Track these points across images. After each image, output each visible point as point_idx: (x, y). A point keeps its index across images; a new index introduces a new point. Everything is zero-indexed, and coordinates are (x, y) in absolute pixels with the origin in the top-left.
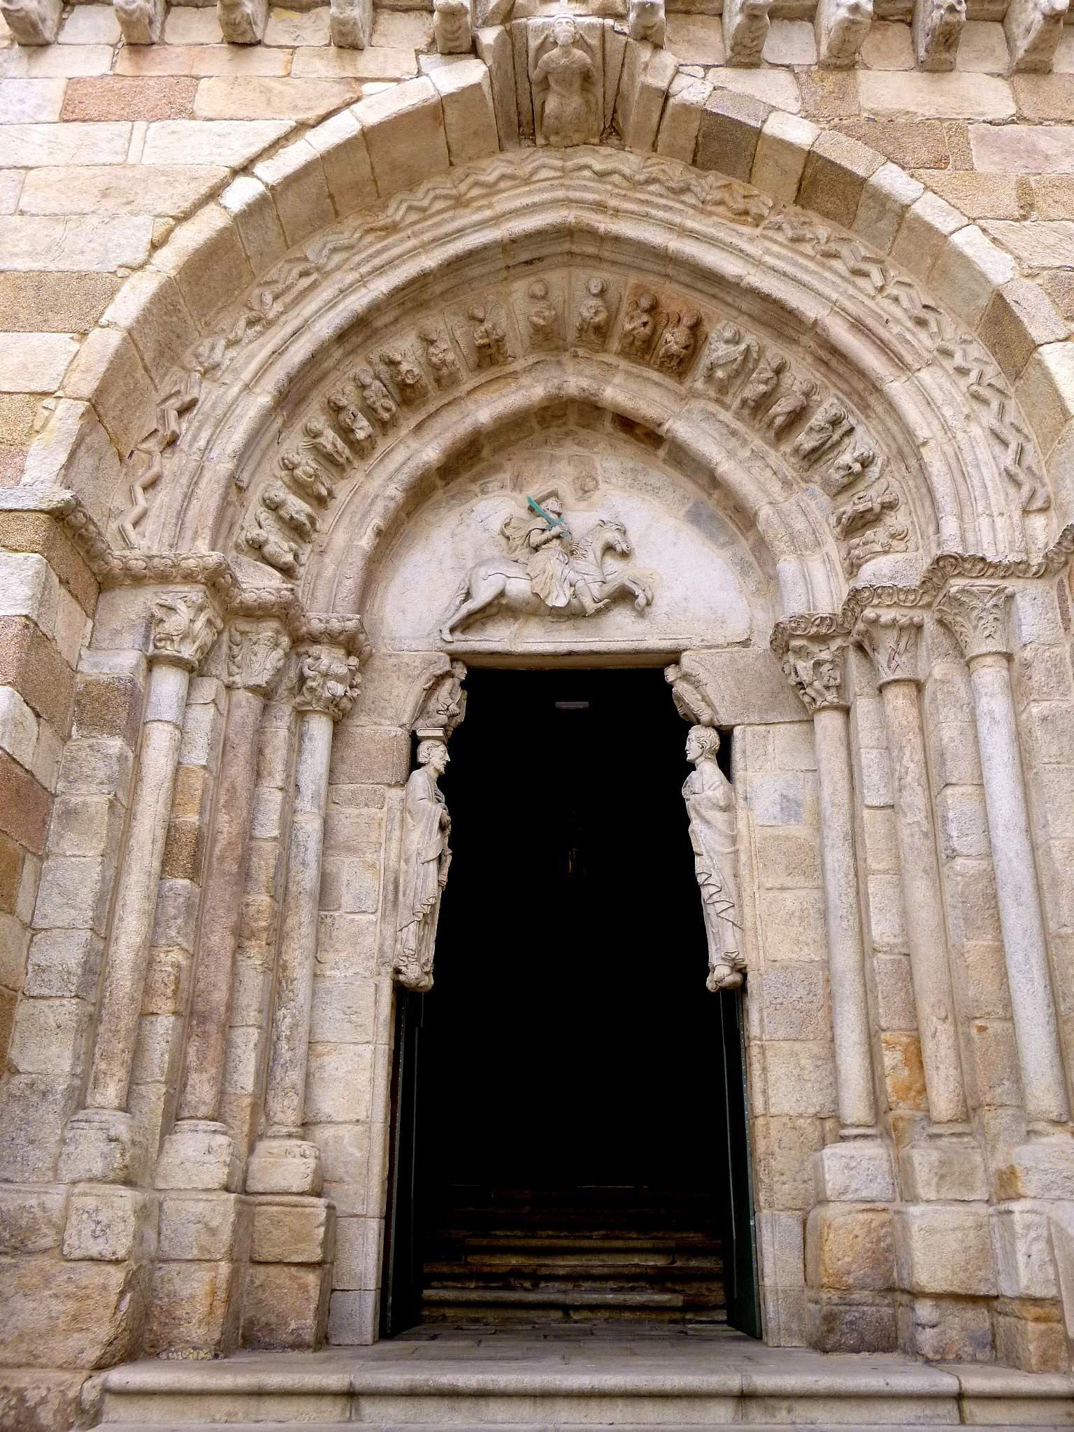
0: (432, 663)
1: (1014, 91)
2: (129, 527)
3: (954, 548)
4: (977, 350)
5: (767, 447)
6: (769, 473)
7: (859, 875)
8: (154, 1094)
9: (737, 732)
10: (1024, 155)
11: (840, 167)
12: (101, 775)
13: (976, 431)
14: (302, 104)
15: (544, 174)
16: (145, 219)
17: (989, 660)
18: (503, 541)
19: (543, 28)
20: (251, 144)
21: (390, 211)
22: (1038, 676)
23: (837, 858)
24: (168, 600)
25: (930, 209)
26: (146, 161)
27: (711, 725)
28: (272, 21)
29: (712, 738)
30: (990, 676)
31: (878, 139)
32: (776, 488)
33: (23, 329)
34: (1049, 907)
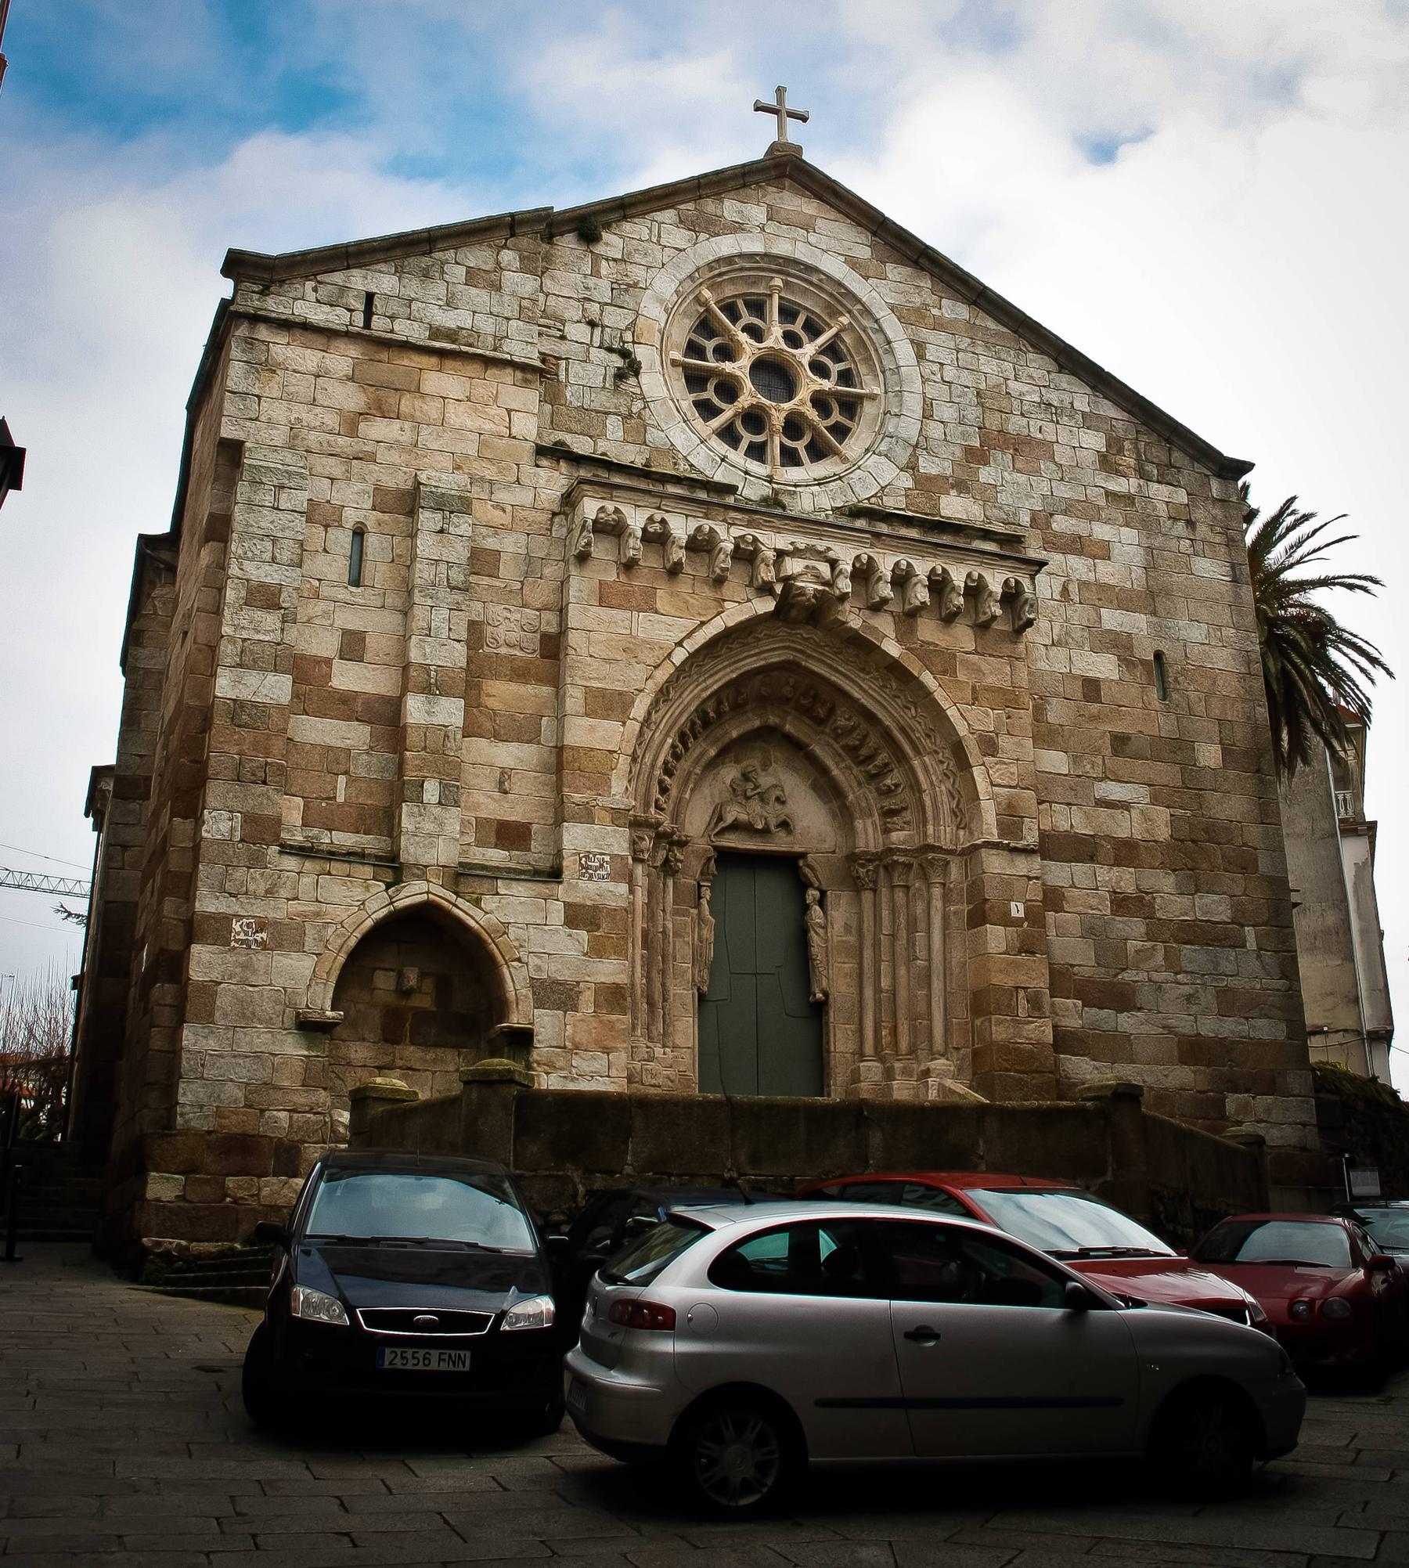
0: (706, 851)
3: (931, 841)
5: (853, 765)
6: (852, 776)
7: (877, 961)
9: (829, 893)
13: (943, 788)
15: (781, 634)
17: (937, 885)
18: (731, 790)
20: (682, 632)
21: (719, 648)
23: (868, 954)
24: (640, 834)
25: (939, 695)
26: (641, 635)
27: (817, 889)
29: (817, 893)
30: (937, 891)
32: (855, 784)
33: (600, 718)
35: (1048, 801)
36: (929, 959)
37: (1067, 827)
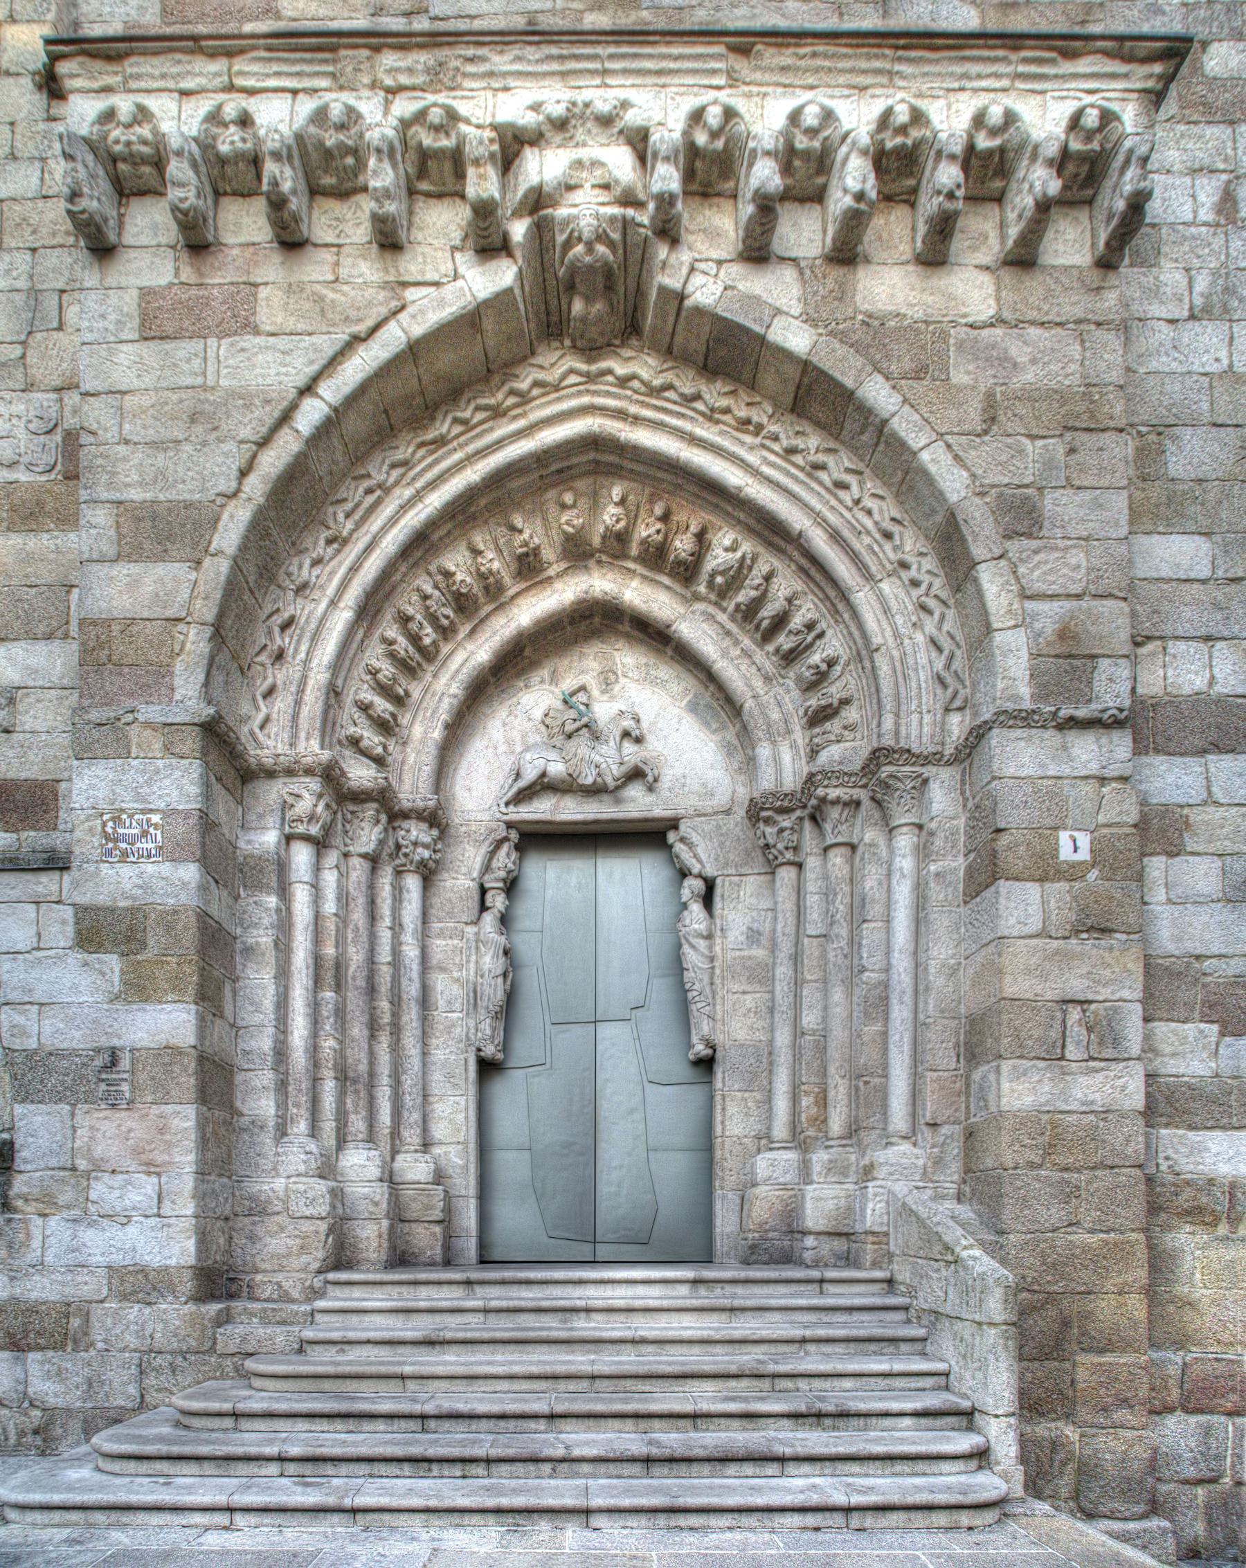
1: (998, 290)
2: (257, 730)
4: (929, 563)
8: (328, 1126)
10: (996, 363)
11: (832, 378)
12: (266, 922)
14: (353, 314)
16: (230, 446)
19: (567, 221)
20: (312, 362)
22: (938, 842)
25: (907, 427)
26: (224, 382)
28: (316, 213)
31: (869, 346)
34: (921, 1005)
35: (1161, 638)
36: (887, 969)
37: (1199, 682)
